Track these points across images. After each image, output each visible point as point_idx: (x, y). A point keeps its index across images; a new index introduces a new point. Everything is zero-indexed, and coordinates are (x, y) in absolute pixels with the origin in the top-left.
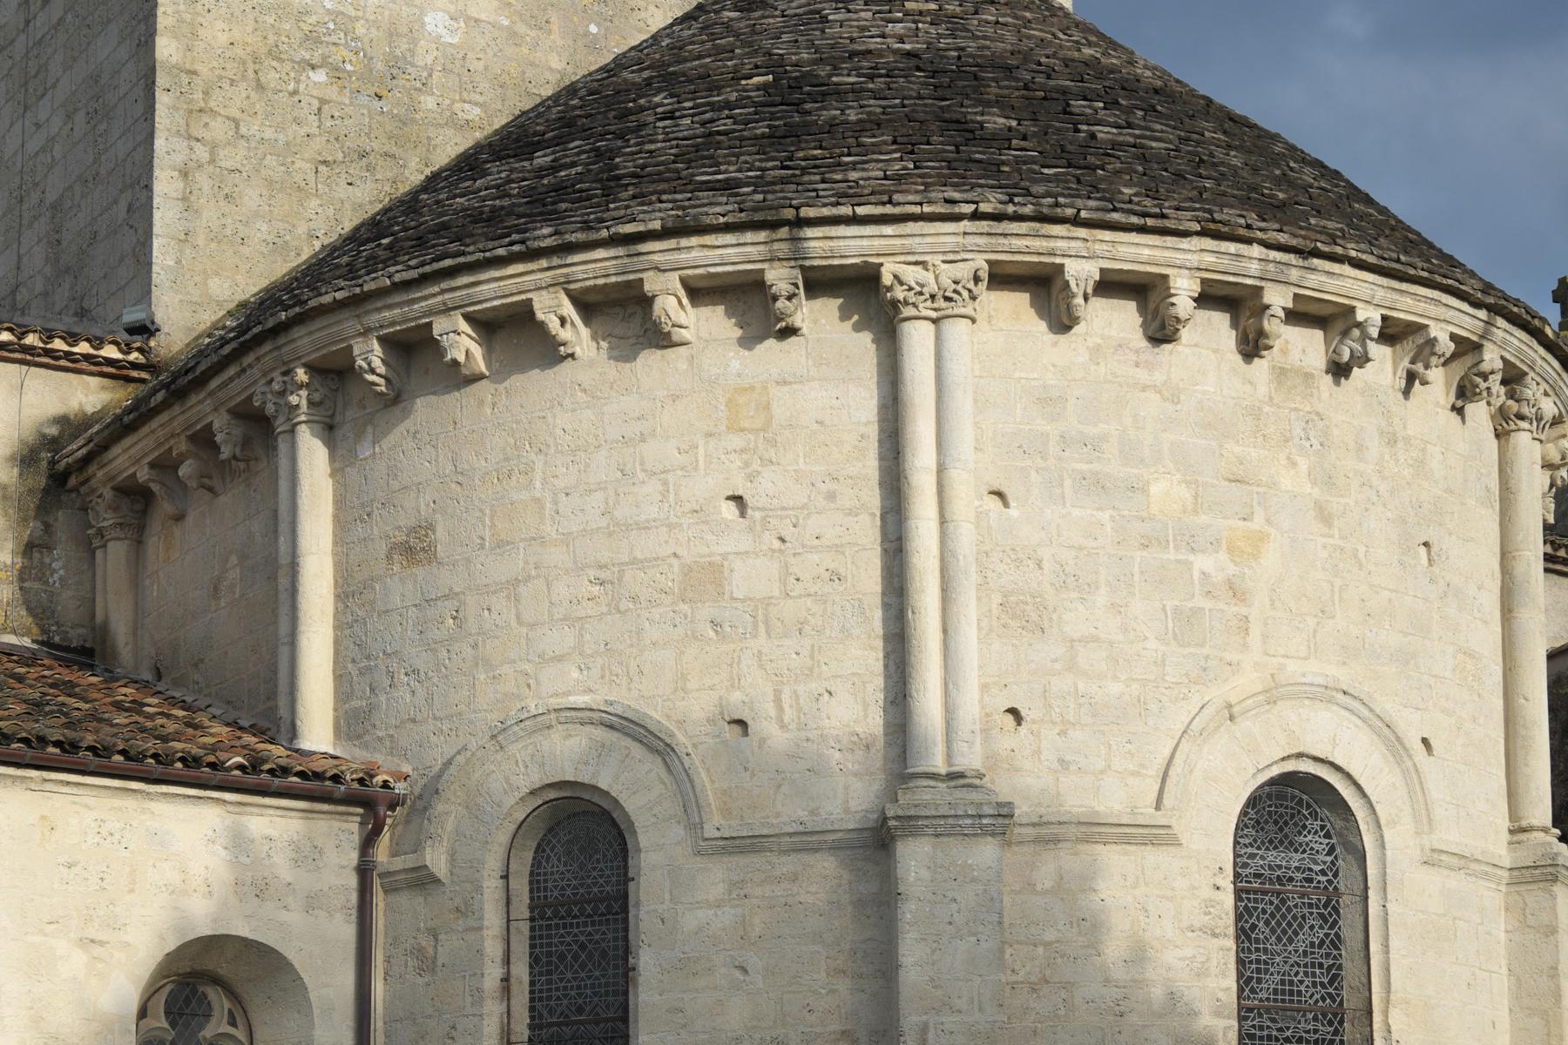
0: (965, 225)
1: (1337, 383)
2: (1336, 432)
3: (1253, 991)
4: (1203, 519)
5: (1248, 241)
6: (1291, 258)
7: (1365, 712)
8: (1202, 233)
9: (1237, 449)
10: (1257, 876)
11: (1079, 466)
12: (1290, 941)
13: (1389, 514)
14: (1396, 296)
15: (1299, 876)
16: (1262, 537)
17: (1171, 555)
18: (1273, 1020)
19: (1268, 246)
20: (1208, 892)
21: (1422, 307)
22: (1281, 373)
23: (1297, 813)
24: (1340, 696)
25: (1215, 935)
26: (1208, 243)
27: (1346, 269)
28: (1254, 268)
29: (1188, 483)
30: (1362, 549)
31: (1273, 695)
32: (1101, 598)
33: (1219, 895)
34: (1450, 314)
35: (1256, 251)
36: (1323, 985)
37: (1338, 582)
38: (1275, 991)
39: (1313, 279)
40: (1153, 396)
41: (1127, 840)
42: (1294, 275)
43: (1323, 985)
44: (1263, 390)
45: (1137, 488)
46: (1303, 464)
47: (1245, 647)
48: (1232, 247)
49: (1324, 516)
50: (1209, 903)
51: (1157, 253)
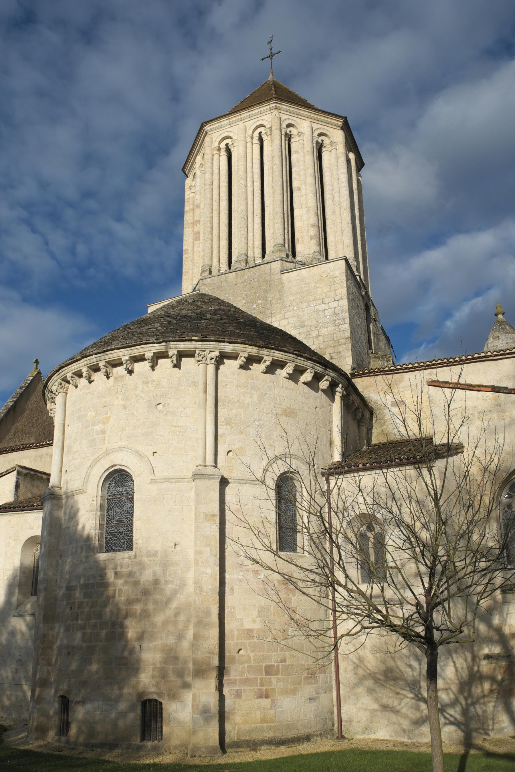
0: (56, 374)
1: (131, 375)
2: (129, 387)
3: (112, 522)
4: (97, 418)
5: (92, 355)
6: (102, 354)
7: (130, 451)
8: (83, 358)
9: (105, 400)
10: (114, 495)
11: (77, 415)
12: (122, 508)
13: (144, 401)
14: (131, 351)
15: (125, 493)
16: (109, 417)
17: (90, 428)
18: (116, 528)
19: (96, 354)
20: (91, 502)
21: (140, 350)
22: (116, 378)
23: (118, 480)
24: (123, 449)
25: (91, 512)
26: (85, 359)
27: (116, 351)
28: (94, 360)
29: (94, 411)
30: (135, 412)
31: (107, 453)
32: (78, 442)
33: (94, 502)
34: (150, 349)
35: (94, 356)
36: (129, 518)
37: (127, 422)
38: (117, 521)
39: (107, 357)
40: (89, 395)
41: (78, 494)
42: (103, 358)
43: (129, 518)
44: (111, 384)
45: (85, 416)
46: (120, 397)
47: (104, 444)
48: (89, 358)
49: (125, 407)
50: (91, 504)
51: (77, 366)
